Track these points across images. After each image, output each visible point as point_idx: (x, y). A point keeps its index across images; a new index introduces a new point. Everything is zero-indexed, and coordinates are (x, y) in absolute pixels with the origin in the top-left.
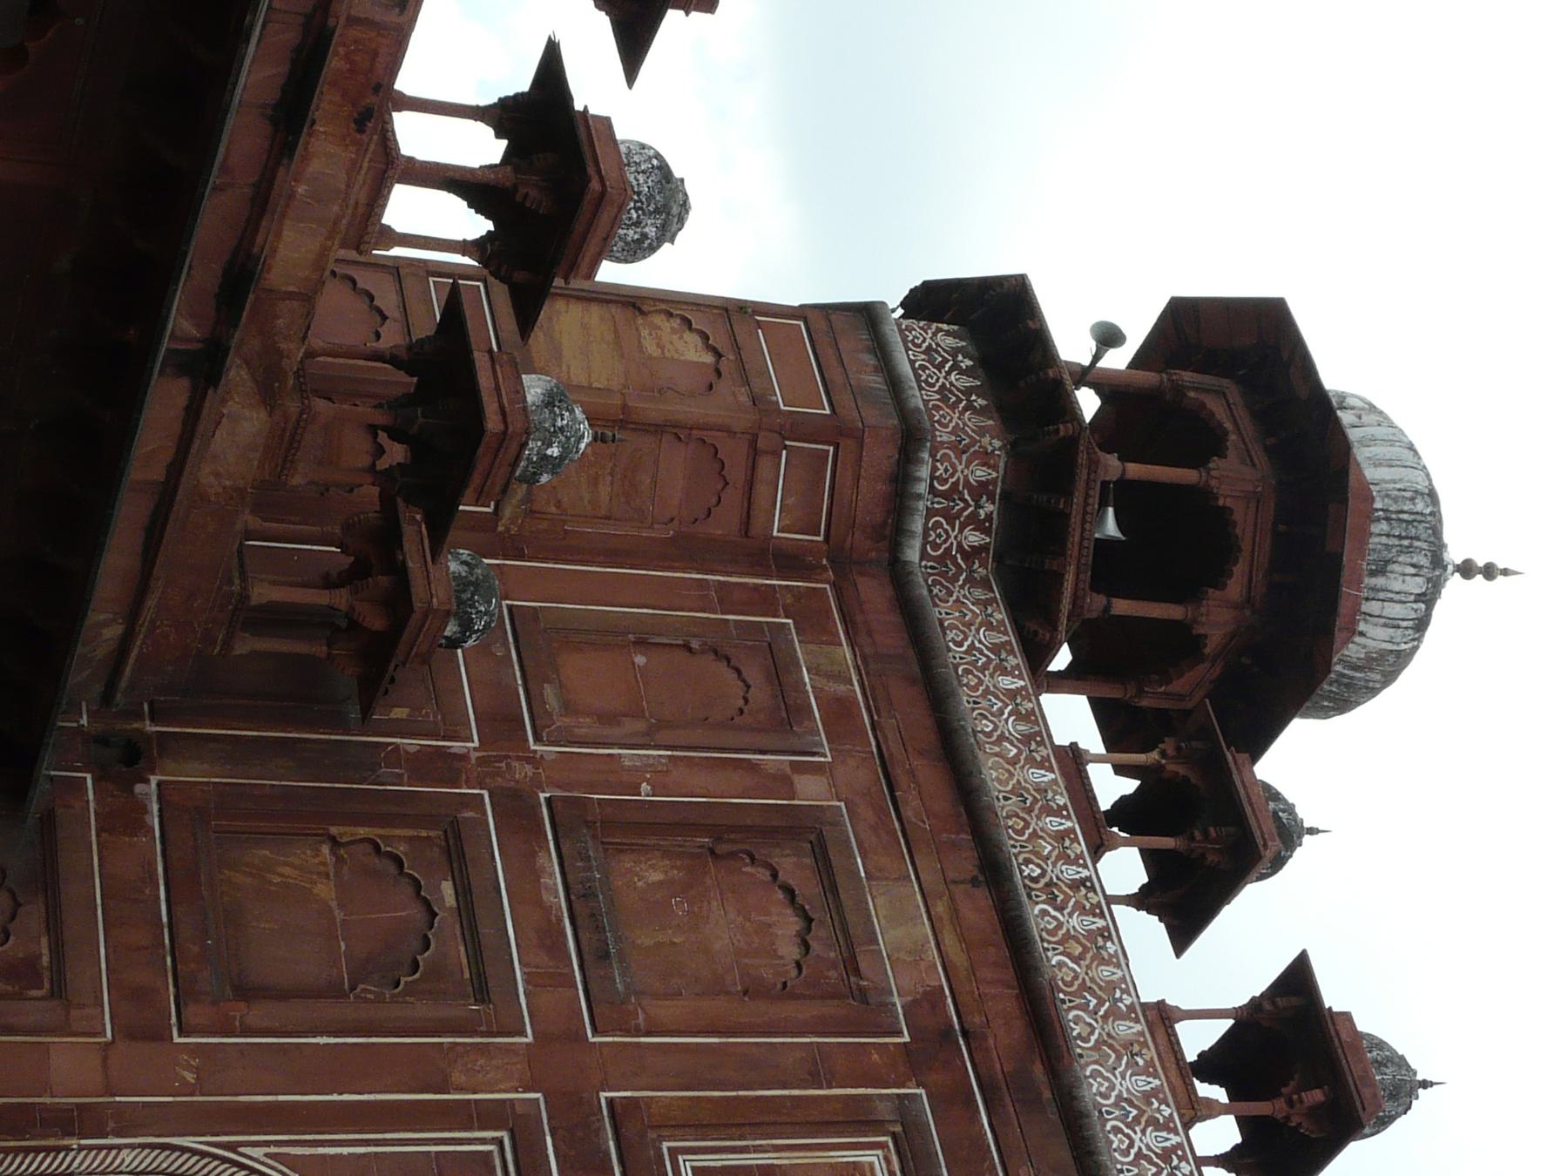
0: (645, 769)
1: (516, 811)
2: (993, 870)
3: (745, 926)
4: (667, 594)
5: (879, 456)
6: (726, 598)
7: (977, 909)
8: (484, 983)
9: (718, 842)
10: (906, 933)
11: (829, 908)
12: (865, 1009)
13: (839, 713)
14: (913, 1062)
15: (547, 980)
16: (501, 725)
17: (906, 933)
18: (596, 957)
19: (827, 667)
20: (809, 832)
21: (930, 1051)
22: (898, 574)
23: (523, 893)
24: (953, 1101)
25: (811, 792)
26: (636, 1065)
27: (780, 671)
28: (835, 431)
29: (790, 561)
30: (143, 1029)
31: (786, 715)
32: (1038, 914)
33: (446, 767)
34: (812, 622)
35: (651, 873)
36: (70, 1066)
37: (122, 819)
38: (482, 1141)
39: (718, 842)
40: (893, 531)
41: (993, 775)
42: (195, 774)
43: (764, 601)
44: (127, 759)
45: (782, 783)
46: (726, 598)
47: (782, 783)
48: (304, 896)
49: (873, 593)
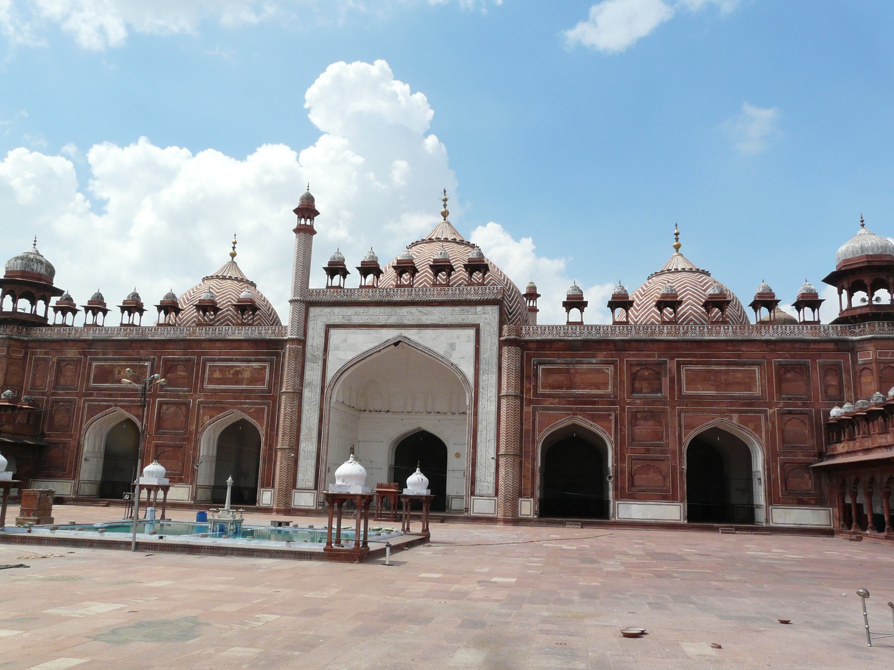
0: (51, 378)
1: (53, 394)
2: (66, 341)
3: (69, 371)
4: (29, 371)
5: (12, 342)
6: (30, 363)
7: (71, 344)
8: (71, 401)
9: (59, 372)
10: (72, 353)
11: (70, 361)
12: (80, 360)
13: (46, 353)
14: (86, 356)
15: (71, 394)
16: (43, 394)
17: (72, 353)
18: (70, 389)
19: (40, 353)
20: (59, 362)
21: (85, 354)
22: (28, 341)
23: (62, 395)
24: (90, 353)
25: (55, 360)
26: (82, 387)
27: (40, 359)
28: (9, 347)
29: (26, 354)
30: (71, 436)
31: (45, 360)
32: (72, 337)
33: (48, 401)
34: (34, 354)
35: (62, 381)
36: (73, 443)
37: (50, 436)
38: (86, 405)
39: (59, 372)
40: (23, 341)
41: (55, 337)
42: (46, 428)
43: (31, 359)
44: (43, 435)
45: (53, 363)
46: (30, 363)
47: (53, 363)
48: (60, 418)
49: (31, 345)
